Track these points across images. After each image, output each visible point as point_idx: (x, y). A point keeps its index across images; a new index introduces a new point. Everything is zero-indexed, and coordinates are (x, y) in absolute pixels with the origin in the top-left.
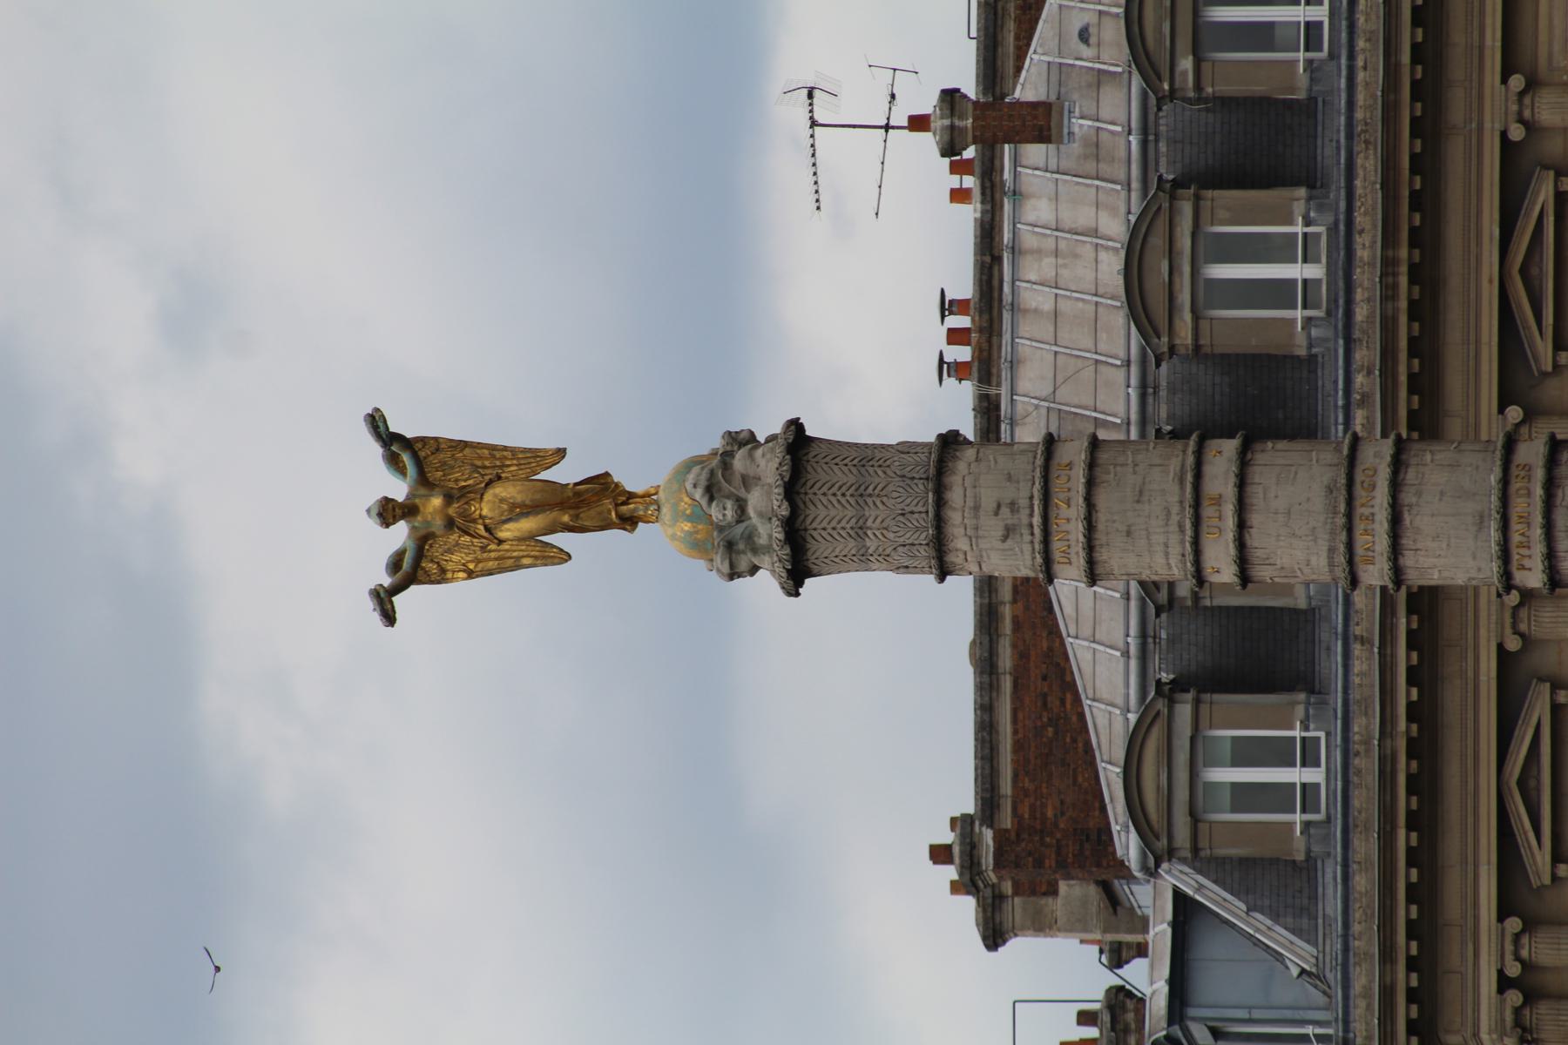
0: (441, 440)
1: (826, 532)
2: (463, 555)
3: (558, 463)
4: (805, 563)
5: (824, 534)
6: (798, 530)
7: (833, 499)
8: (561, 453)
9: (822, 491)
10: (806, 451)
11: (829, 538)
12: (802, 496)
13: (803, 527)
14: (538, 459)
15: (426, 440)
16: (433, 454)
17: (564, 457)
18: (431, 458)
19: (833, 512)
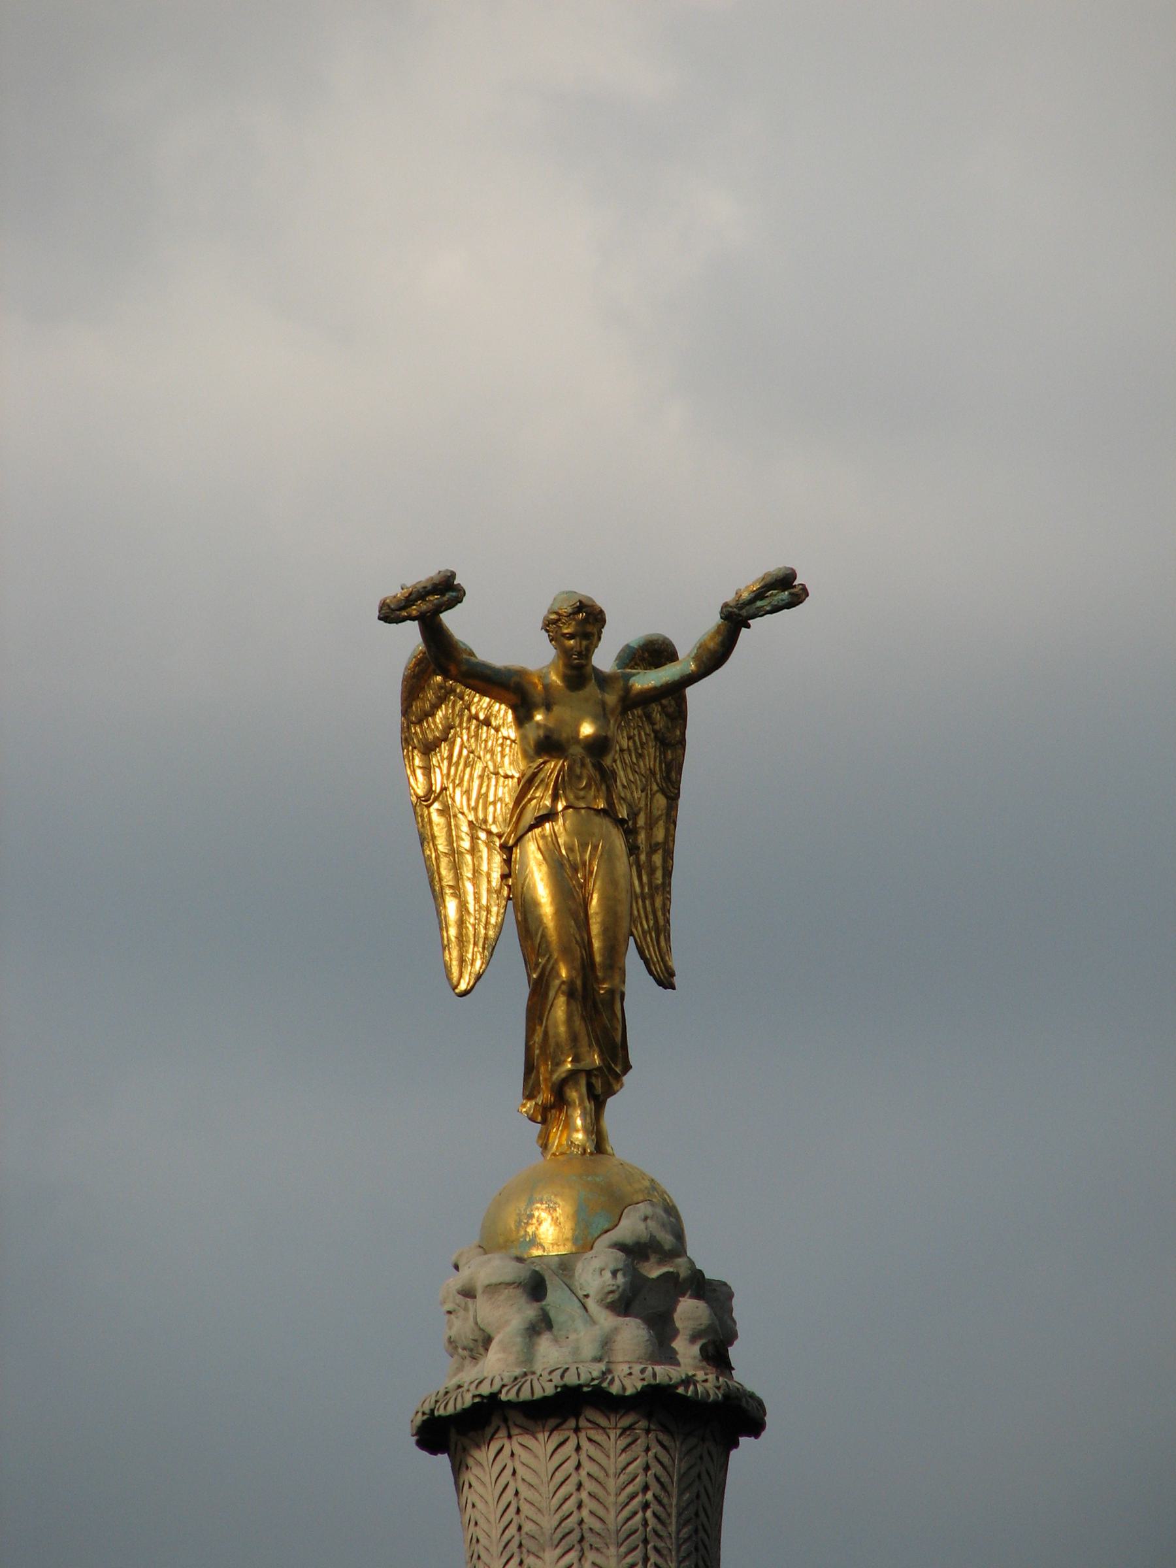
0: (680, 752)
3: (651, 973)
4: (502, 1433)
11: (560, 1476)
12: (643, 1424)
17: (660, 983)
19: (612, 1484)
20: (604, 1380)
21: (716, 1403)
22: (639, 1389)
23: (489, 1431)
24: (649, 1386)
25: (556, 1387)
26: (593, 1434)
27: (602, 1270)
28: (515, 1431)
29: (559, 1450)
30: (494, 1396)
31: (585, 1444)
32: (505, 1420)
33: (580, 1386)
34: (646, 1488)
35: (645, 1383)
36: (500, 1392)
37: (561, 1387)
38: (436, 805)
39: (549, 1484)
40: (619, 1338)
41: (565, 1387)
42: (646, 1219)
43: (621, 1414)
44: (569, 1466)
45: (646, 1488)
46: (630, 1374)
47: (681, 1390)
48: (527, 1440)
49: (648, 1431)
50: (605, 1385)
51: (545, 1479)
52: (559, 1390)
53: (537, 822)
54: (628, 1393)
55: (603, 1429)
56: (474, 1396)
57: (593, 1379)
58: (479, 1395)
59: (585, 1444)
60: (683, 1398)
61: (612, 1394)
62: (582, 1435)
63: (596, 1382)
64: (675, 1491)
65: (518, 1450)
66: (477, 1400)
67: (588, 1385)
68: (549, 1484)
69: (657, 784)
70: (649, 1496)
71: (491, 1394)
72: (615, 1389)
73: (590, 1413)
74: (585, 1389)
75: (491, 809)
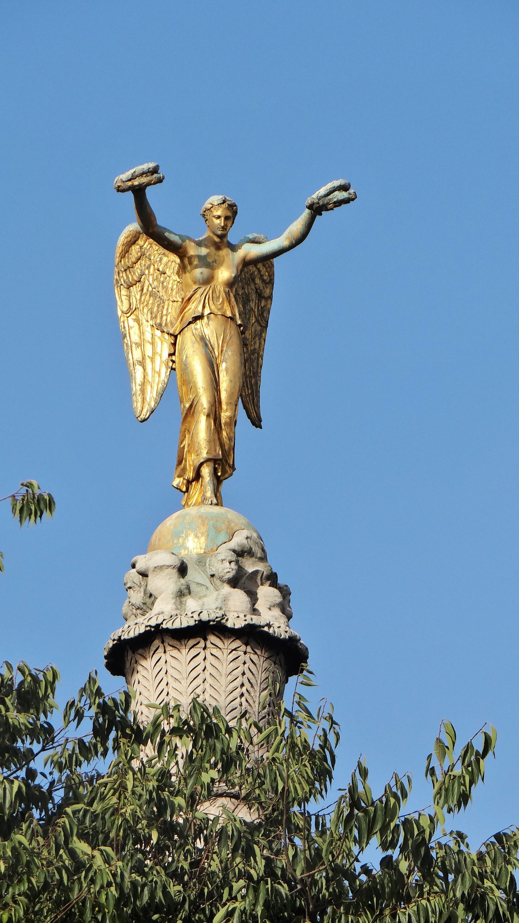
0: (269, 302)
1: (201, 671)
2: (150, 306)
4: (161, 650)
5: (200, 669)
6: (205, 639)
7: (238, 683)
8: (257, 422)
9: (247, 672)
10: (283, 665)
11: (194, 674)
12: (243, 648)
13: (209, 644)
14: (251, 397)
15: (269, 286)
16: (257, 289)
17: (254, 424)
18: (253, 286)
19: (223, 681)
20: (223, 619)
21: (284, 640)
22: (243, 626)
23: (153, 648)
24: (248, 624)
25: (195, 621)
26: (215, 651)
27: (222, 560)
28: (168, 648)
29: (193, 660)
30: (158, 626)
31: (209, 657)
32: (163, 642)
33: (209, 621)
34: (242, 685)
35: (247, 623)
36: (162, 623)
37: (198, 621)
38: (133, 317)
39: (187, 679)
40: (231, 599)
41: (200, 621)
42: (247, 538)
43: (232, 640)
44: (200, 669)
45: (242, 685)
46: (238, 617)
47: (266, 629)
48: (175, 653)
49: (245, 653)
50: (224, 621)
51: (185, 675)
52: (197, 622)
53: (193, 320)
54: (236, 627)
55: (220, 649)
56: (146, 626)
57: (217, 618)
58: (150, 626)
59: (209, 657)
60: (267, 634)
61: (228, 627)
62: (208, 652)
63: (218, 619)
64: (257, 688)
65: (169, 659)
66: (148, 628)
67: (214, 621)
68: (187, 679)
69: (256, 317)
70: (244, 689)
71: (157, 624)
72: (229, 624)
73: (212, 638)
74: (211, 623)
75: (164, 318)
